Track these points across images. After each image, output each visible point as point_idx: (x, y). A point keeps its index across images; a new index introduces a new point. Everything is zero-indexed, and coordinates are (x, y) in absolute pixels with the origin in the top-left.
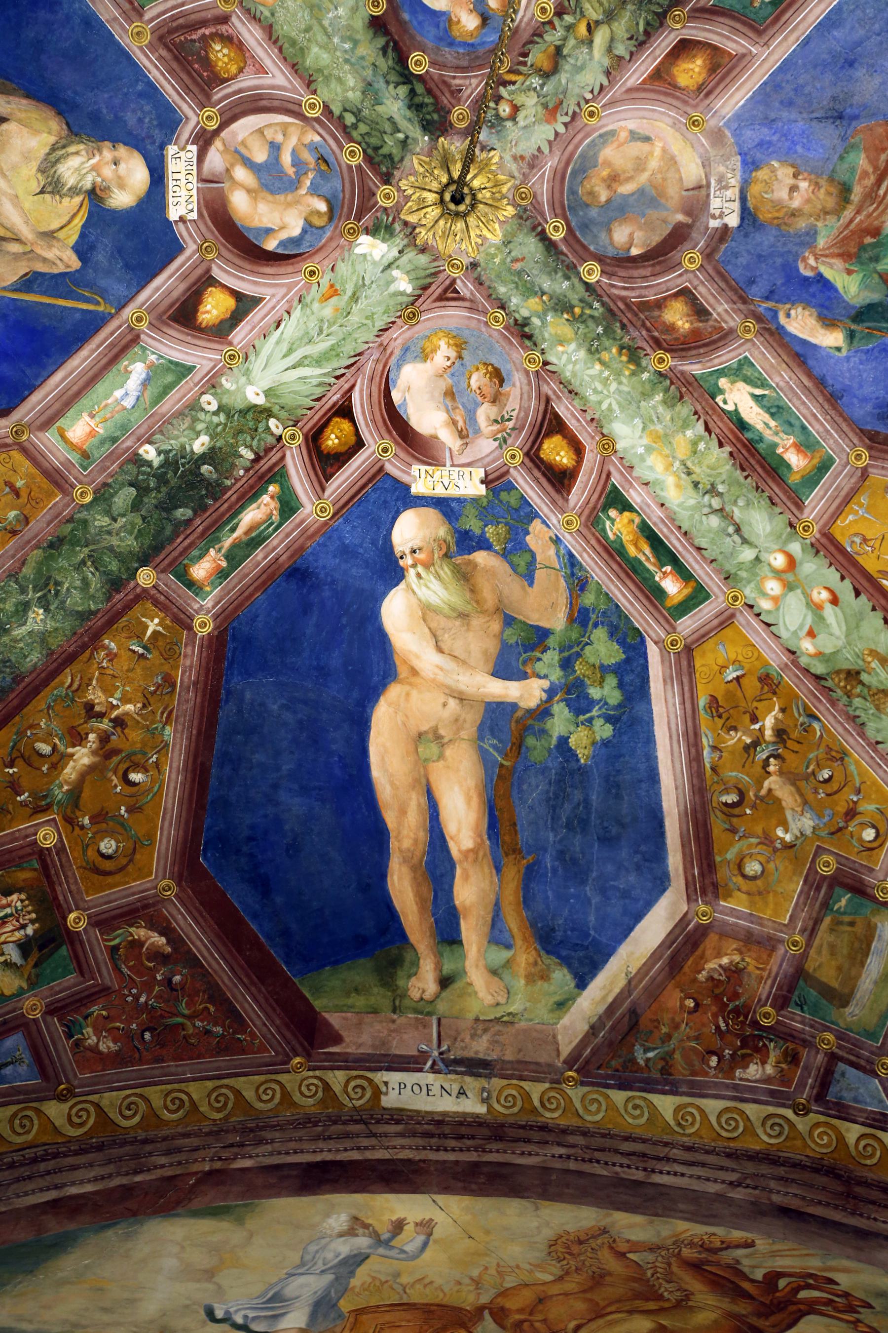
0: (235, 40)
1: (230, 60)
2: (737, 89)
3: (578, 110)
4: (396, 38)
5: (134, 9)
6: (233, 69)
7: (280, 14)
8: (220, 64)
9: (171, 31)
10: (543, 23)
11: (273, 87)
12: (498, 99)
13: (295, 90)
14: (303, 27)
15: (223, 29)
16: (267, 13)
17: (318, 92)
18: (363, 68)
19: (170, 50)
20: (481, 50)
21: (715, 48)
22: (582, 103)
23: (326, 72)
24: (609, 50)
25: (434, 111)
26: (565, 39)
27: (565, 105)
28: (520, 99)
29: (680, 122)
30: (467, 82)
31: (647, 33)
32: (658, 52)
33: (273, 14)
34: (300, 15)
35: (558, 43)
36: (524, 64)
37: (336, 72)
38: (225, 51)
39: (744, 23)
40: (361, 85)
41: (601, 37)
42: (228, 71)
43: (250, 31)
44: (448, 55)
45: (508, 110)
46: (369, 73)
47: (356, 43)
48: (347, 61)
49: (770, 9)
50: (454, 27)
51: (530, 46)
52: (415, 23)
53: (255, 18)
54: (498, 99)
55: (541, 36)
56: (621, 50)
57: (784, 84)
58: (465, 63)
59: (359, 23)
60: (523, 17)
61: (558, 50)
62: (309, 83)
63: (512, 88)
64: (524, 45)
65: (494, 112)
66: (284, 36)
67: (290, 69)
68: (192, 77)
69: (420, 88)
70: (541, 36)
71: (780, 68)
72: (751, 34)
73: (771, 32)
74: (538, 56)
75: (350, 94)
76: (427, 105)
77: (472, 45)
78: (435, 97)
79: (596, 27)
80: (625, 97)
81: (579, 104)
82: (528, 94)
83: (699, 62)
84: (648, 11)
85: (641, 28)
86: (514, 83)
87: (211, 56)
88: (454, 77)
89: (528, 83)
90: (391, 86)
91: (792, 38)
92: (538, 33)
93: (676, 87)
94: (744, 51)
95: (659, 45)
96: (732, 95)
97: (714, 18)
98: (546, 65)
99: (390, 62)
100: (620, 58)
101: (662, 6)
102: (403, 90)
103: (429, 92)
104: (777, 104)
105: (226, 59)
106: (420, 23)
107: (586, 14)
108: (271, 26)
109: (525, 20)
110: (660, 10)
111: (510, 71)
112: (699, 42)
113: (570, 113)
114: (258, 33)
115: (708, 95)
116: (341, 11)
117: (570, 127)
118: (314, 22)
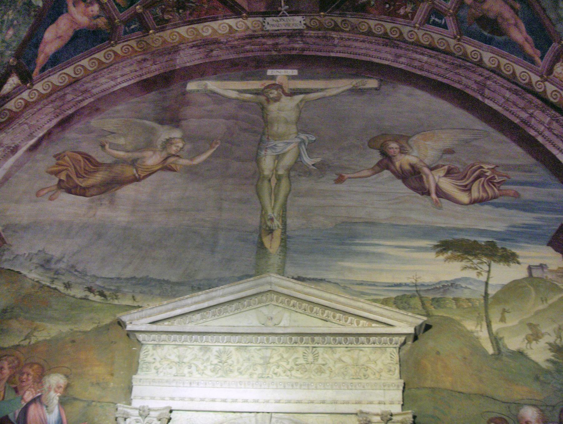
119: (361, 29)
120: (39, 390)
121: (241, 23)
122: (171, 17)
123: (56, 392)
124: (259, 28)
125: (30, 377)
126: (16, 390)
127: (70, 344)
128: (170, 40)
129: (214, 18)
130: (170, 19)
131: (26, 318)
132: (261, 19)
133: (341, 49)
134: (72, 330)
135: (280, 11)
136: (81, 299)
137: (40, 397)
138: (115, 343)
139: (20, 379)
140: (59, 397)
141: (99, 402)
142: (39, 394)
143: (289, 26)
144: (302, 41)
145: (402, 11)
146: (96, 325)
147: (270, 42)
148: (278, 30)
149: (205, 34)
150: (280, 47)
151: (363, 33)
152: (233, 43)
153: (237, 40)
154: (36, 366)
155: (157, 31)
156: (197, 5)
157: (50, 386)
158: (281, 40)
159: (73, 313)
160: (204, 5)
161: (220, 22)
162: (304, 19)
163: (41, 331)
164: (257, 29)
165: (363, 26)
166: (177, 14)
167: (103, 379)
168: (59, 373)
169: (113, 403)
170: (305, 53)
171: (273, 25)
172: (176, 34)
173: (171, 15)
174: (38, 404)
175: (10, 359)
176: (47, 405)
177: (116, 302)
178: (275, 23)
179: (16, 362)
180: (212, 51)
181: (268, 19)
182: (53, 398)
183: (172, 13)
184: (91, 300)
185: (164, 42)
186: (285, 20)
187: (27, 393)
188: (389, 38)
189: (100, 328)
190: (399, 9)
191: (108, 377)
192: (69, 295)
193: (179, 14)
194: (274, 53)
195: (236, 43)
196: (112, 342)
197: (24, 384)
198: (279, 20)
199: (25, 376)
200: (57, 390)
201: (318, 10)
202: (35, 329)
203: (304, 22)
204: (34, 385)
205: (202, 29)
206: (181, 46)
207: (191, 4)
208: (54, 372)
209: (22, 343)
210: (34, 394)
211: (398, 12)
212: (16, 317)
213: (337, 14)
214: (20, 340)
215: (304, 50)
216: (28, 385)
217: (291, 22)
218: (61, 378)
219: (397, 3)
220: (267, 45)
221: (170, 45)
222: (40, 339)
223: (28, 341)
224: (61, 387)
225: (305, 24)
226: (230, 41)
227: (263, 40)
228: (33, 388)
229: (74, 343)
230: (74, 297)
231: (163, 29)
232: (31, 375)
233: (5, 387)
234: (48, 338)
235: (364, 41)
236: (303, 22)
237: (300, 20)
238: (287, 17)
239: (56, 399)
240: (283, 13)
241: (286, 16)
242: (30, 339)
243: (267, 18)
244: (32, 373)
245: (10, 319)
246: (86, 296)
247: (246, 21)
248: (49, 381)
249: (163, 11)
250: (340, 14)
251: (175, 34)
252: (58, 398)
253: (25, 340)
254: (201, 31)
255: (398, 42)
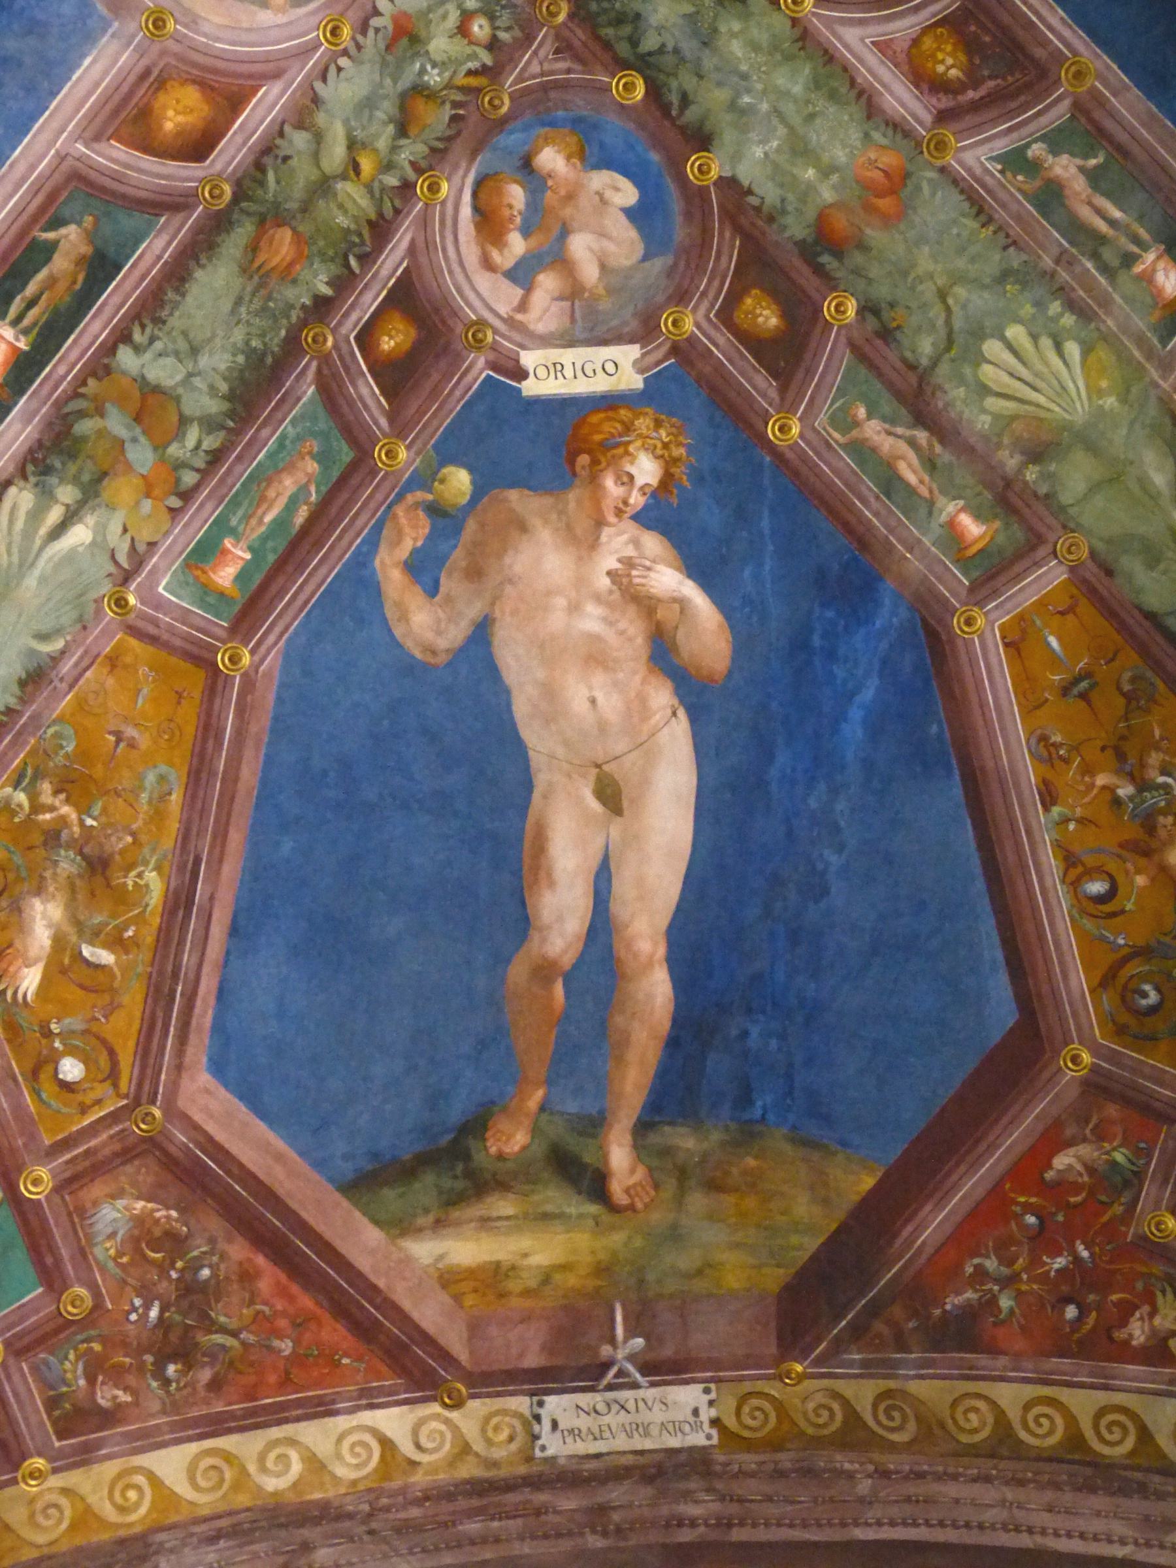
0: (925, 87)
1: (933, 56)
2: (97, 85)
3: (359, 38)
4: (666, 123)
5: (1087, 113)
6: (928, 43)
7: (855, 136)
8: (949, 48)
9: (1028, 86)
10: (431, 168)
11: (862, 22)
12: (493, 45)
13: (829, 22)
14: (818, 121)
15: (945, 102)
16: (876, 136)
17: (789, 23)
18: (718, 69)
19: (1032, 59)
20: (528, 117)
21: (147, 149)
22: (353, 51)
23: (778, 57)
24: (319, 137)
25: (598, 14)
26: (394, 149)
27: (382, 45)
28: (458, 47)
29: (186, 26)
30: (546, 66)
31: (259, 167)
32: (239, 139)
33: (867, 135)
34: (824, 138)
35: (403, 142)
36: (456, 105)
37: (761, 59)
38: (941, 69)
39: (104, 189)
40: (721, 42)
41: (336, 153)
42: (937, 38)
43: (903, 105)
44: (581, 105)
45: (476, 28)
46: (709, 62)
47: (733, 106)
48: (745, 77)
49: (66, 212)
50: (574, 148)
51: (449, 133)
52: (639, 148)
53: (896, 127)
54: (493, 45)
55: (433, 150)
56: (300, 140)
57: (21, 94)
58: (553, 95)
59: (728, 137)
60: (465, 176)
61: (402, 130)
62: (803, 35)
63: (472, 65)
64: (459, 133)
65: (498, 23)
66: (847, 103)
67: (837, 55)
68: (995, 21)
69: (623, 49)
70: (433, 150)
71: (33, 119)
72: (93, 175)
73: (58, 177)
74: (437, 119)
75: (736, 26)
76: (610, 24)
77: (543, 124)
78: (597, 38)
79: (345, 171)
80: (282, 64)
81: (359, 47)
82: (444, 57)
83: (169, 126)
84: (263, 202)
85: (271, 176)
86: (470, 73)
87: (962, 58)
88: (569, 71)
89: (447, 74)
90: (670, 47)
91: (21, 168)
92: (438, 154)
93: (201, 84)
94: (96, 146)
95: (239, 150)
96: (106, 73)
97: (152, 196)
98: (420, 106)
99: (674, 84)
100: (300, 126)
101: (242, 210)
102: (650, 43)
103: (607, 46)
104: (28, 60)
105: (940, 56)
106: (632, 147)
107: (363, 190)
108: (869, 117)
109: (461, 172)
110: (244, 205)
111: (478, 90)
112: (174, 158)
113: (371, 33)
114: (889, 103)
115: (146, 73)
116: (759, 152)
117: (369, 7)
118: (801, 131)
119: (962, 1430)
121: (434, 1425)
122: (125, 1397)
124: (514, 1447)
128: (109, 1513)
129: (320, 1401)
130: (119, 1406)
132: (521, 1404)
133: (895, 1511)
135: (606, 1365)
143: (647, 1434)
144: (708, 1491)
145: (1137, 1331)
147: (569, 1502)
148: (598, 1456)
149: (272, 1484)
150: (616, 1517)
151: (974, 1446)
152: (402, 1515)
153: (418, 1502)
155: (64, 1463)
156: (244, 1343)
158: (615, 1494)
160: (276, 1343)
161: (342, 1422)
162: (713, 1396)
164: (498, 1453)
165: (973, 1416)
166: (154, 1384)
170: (738, 1535)
171: (574, 1433)
172: (140, 1479)
173: (126, 1389)
178: (583, 1422)
180: (306, 1547)
181: (555, 1404)
183: (131, 1380)
185: (86, 1517)
186: (631, 1405)
188: (1097, 1464)
190: (1124, 1322)
193: (167, 1382)
194: (595, 1542)
195: (415, 1512)
198: (601, 1407)
201: (773, 1350)
203: (713, 1413)
205: (262, 1459)
206: (161, 1537)
207: (218, 1338)
211: (1120, 1335)
213: (852, 1363)
215: (730, 1526)
217: (657, 1415)
219: (1114, 1297)
220: (556, 1512)
221: (105, 1536)
225: (715, 1422)
226: (387, 1509)
227: (542, 1497)
231: (84, 1457)
235: (988, 1479)
236: (706, 1414)
237: (693, 1405)
238: (641, 1393)
240: (621, 1373)
241: (635, 1386)
243: (551, 1401)
247: (454, 1415)
249: (95, 1368)
250: (865, 1364)
251: (140, 1479)
254: (252, 1468)
255: (1138, 1475)
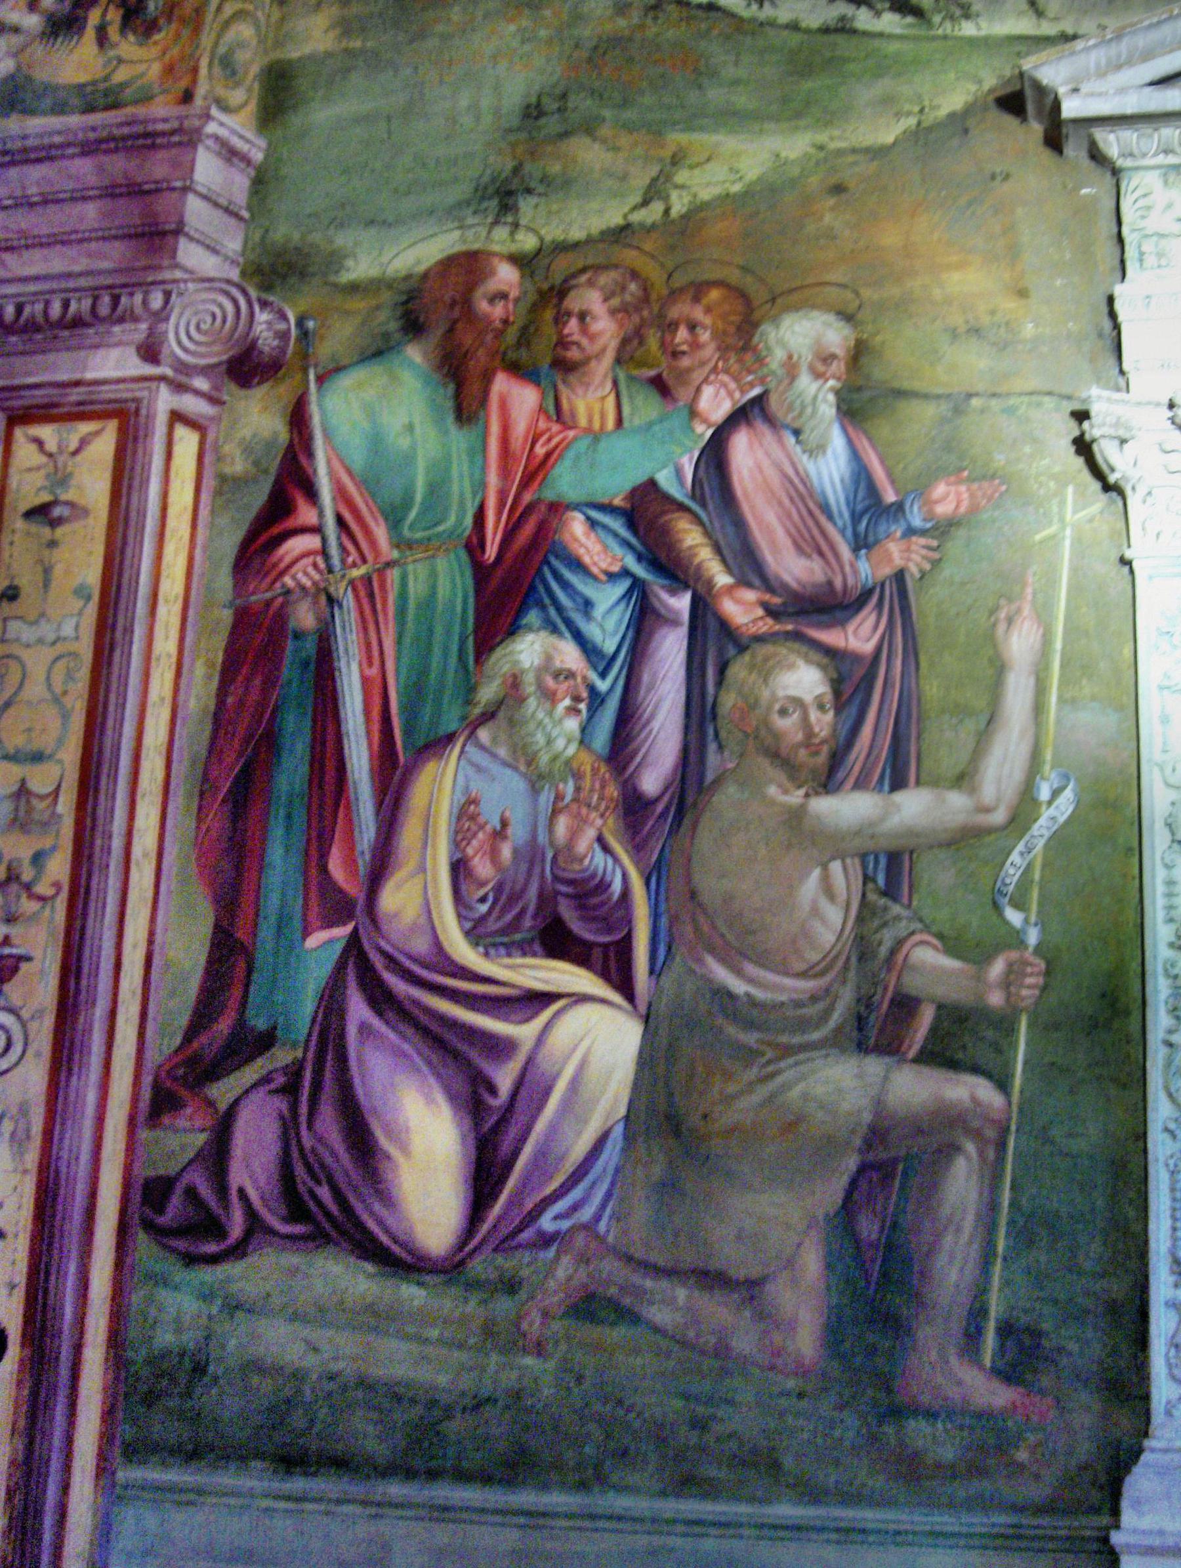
120: (750, 378)
123: (818, 375)
125: (705, 336)
126: (661, 387)
127: (832, 201)
131: (629, 128)
134: (821, 148)
136: (826, 30)
137: (759, 402)
138: (1007, 177)
139: (663, 344)
140: (837, 393)
141: (994, 395)
142: (756, 392)
146: (912, 121)
154: (715, 294)
157: (790, 357)
159: (808, 85)
163: (698, 165)
167: (993, 313)
168: (814, 307)
169: (1049, 393)
174: (761, 426)
175: (606, 279)
176: (796, 425)
177: (968, 29)
179: (633, 287)
182: (815, 398)
184: (865, 34)
187: (708, 392)
189: (930, 129)
191: (1010, 304)
192: (771, 23)
196: (993, 177)
197: (685, 362)
199: (682, 334)
200: (821, 368)
202: (677, 160)
204: (726, 360)
208: (796, 308)
209: (637, 217)
210: (737, 395)
212: (589, 128)
214: (626, 209)
216: (703, 364)
218: (827, 325)
222: (705, 195)
223: (657, 208)
224: (833, 356)
228: (727, 371)
229: (844, 196)
230: (794, 26)
232: (705, 328)
233: (615, 383)
234: (736, 188)
239: (825, 400)
242: (666, 199)
244: (708, 321)
245: (565, 134)
246: (843, 18)
248: (781, 342)
252: (831, 397)
253: (645, 203)
